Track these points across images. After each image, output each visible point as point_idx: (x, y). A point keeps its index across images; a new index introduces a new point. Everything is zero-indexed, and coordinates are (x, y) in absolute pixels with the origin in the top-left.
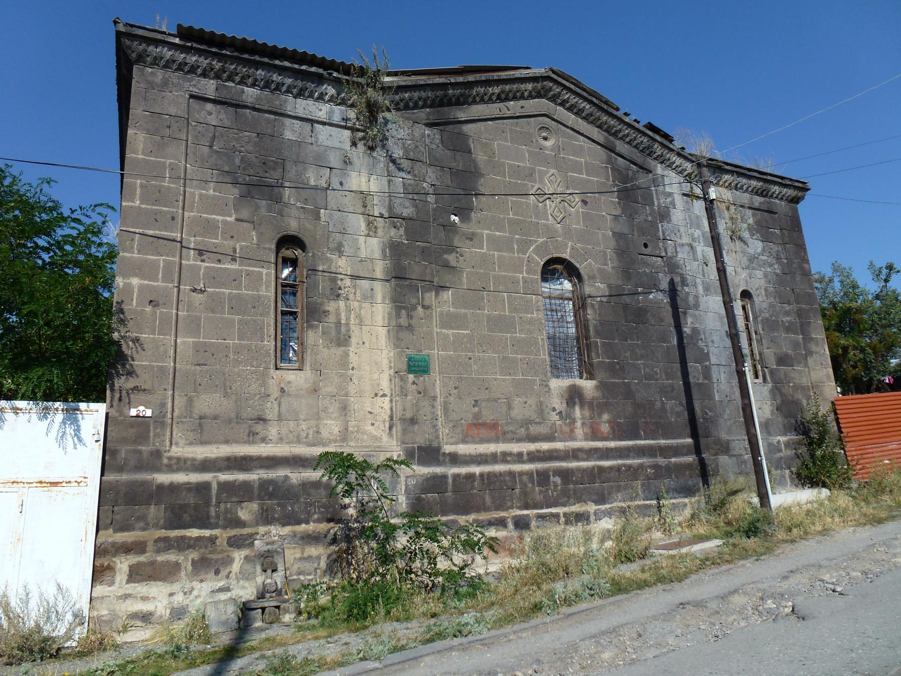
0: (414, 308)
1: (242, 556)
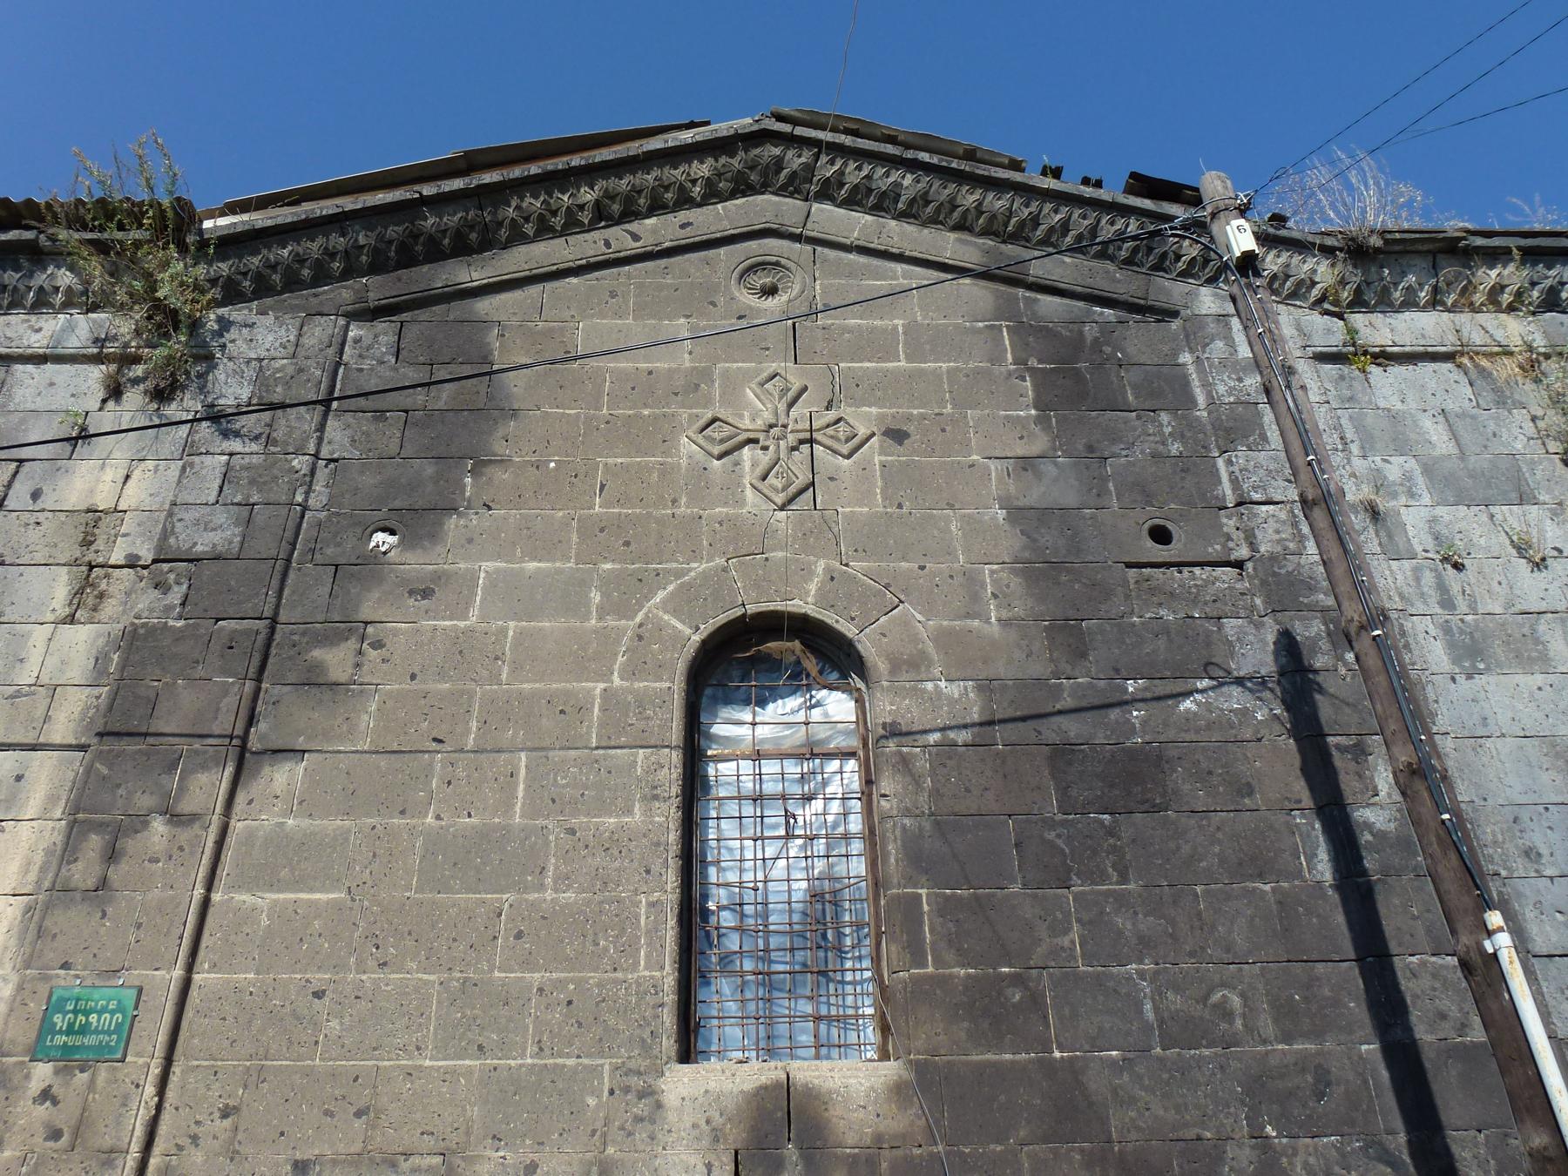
0: (140, 822)
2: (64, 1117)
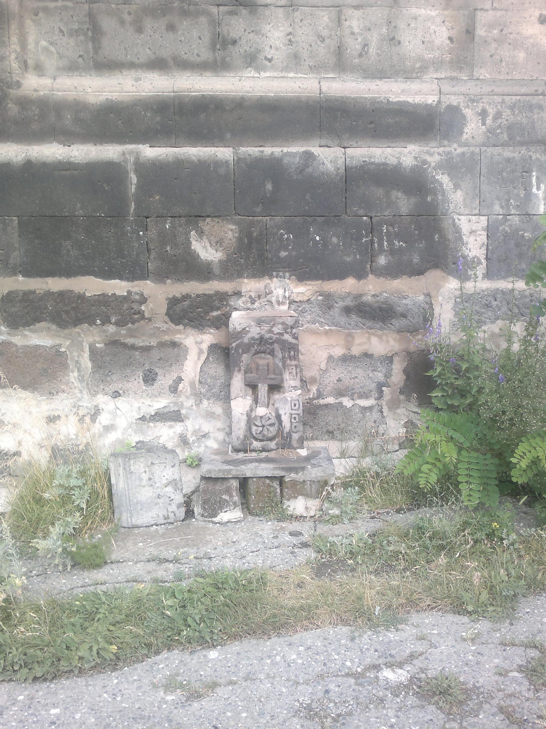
1: (205, 347)
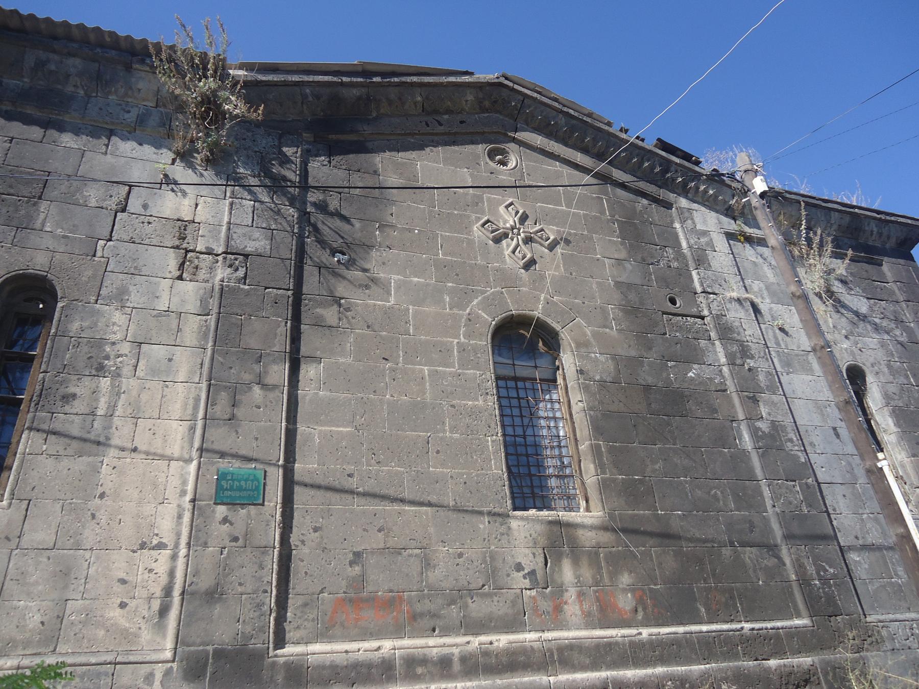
0: (248, 386)
2: (239, 530)
